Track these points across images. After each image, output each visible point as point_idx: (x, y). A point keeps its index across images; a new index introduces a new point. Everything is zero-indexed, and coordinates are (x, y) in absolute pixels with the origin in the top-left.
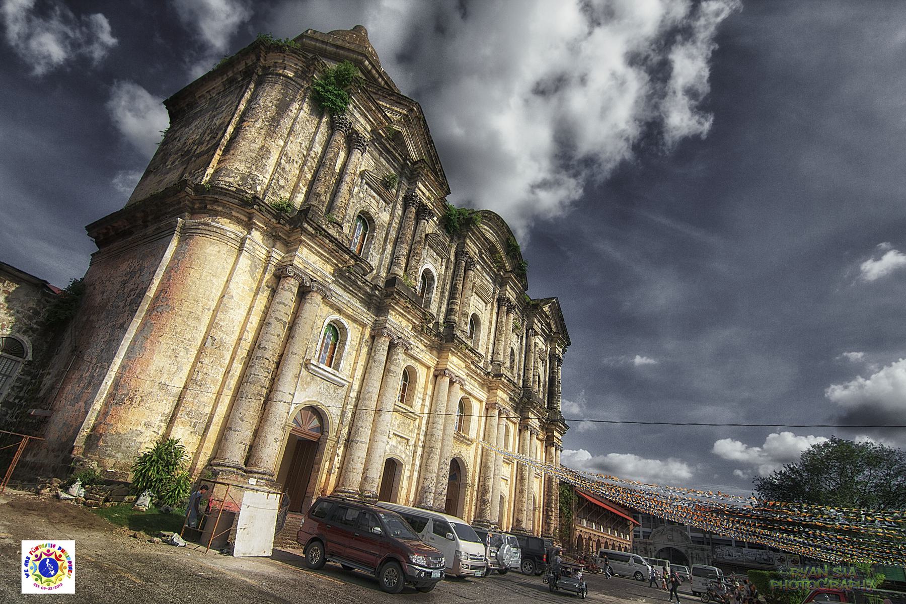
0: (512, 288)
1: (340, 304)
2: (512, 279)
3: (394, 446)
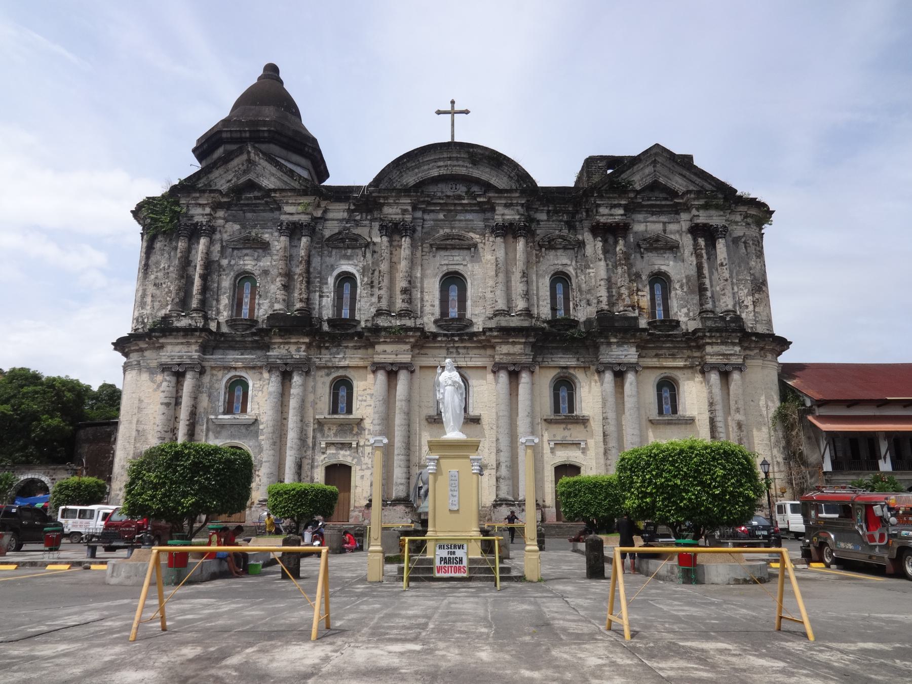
0: (506, 206)
1: (226, 364)
2: (494, 197)
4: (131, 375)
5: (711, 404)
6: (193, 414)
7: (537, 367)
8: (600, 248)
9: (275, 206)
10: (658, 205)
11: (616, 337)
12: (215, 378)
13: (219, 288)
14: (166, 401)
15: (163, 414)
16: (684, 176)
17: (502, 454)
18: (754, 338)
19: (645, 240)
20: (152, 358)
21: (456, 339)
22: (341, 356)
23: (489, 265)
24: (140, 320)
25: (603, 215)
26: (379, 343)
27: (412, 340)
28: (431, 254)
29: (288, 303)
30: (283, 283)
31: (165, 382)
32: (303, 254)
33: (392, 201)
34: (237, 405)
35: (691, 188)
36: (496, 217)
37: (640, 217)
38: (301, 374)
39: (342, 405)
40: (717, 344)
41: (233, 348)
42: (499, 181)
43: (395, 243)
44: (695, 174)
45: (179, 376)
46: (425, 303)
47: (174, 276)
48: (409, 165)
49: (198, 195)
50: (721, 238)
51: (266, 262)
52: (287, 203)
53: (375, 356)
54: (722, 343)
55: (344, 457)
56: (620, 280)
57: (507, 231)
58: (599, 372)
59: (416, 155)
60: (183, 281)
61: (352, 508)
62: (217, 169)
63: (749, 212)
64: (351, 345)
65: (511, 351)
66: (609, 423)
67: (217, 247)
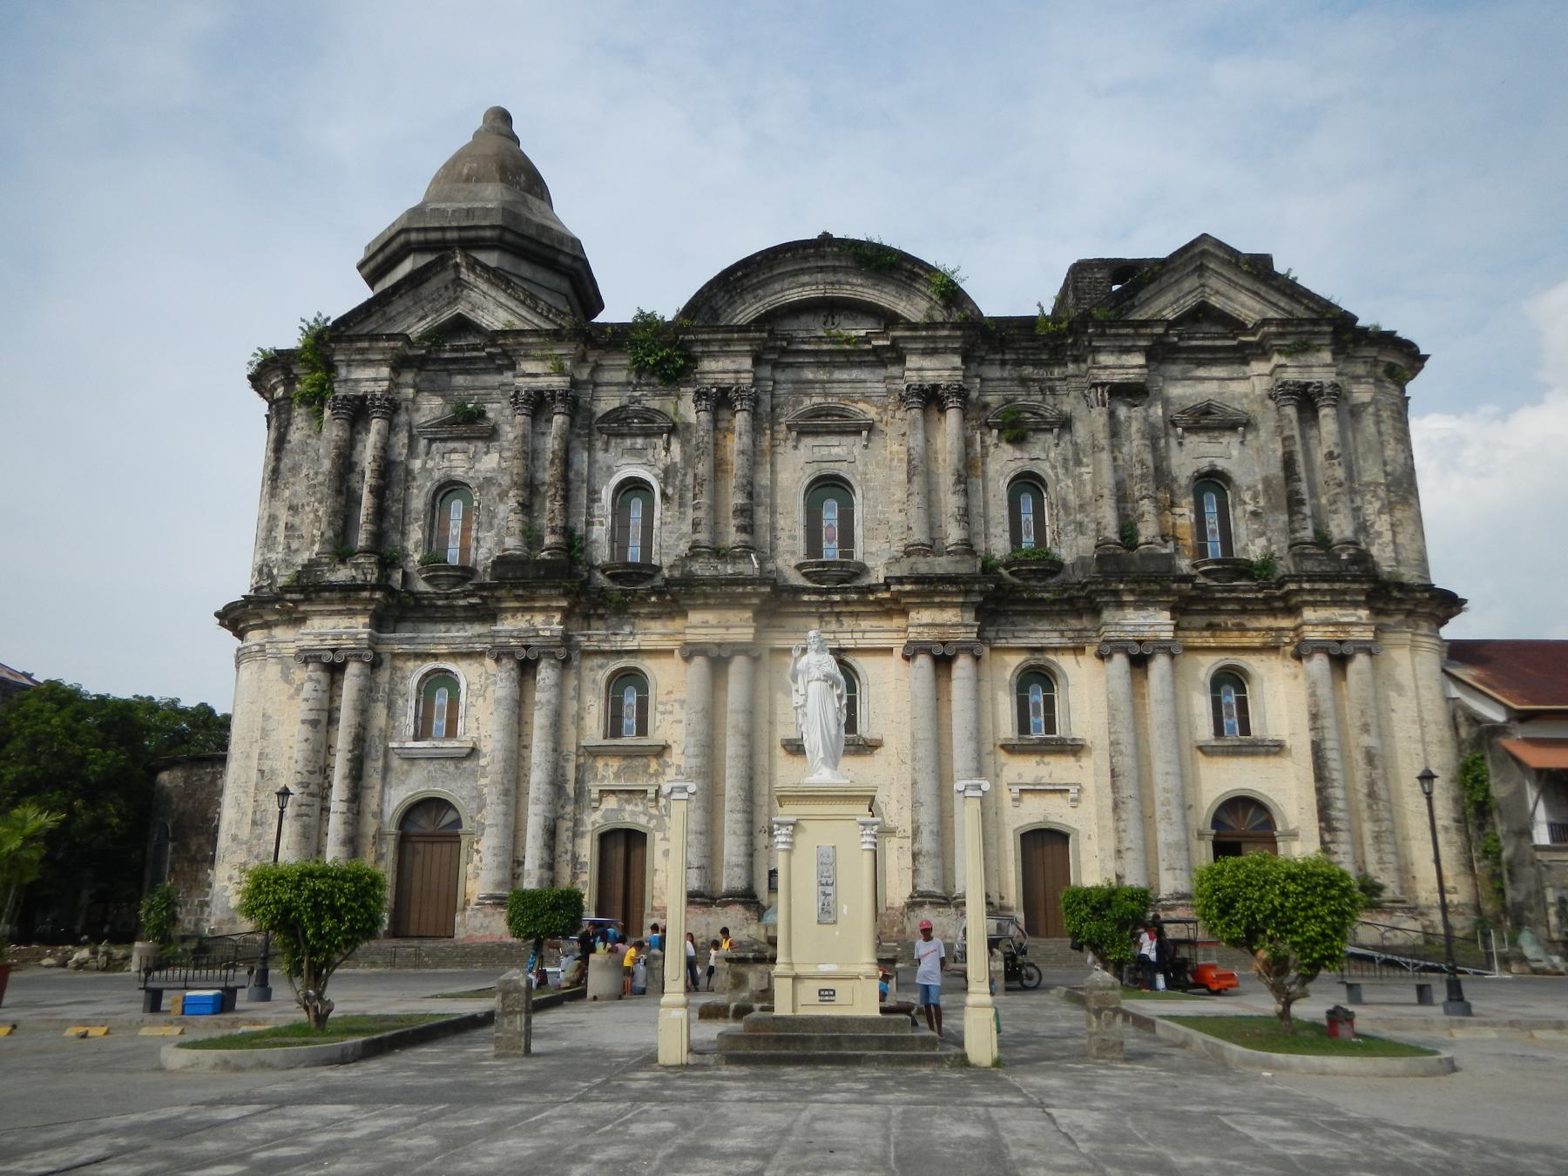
0: (926, 353)
1: (421, 648)
3: (613, 810)
4: (249, 671)
5: (1314, 717)
6: (360, 740)
7: (987, 650)
8: (1101, 428)
9: (506, 362)
10: (1208, 347)
11: (1132, 592)
12: (399, 674)
13: (405, 511)
14: (312, 716)
15: (306, 740)
16: (1257, 294)
17: (922, 809)
18: (1396, 594)
20: (288, 639)
21: (837, 598)
22: (627, 629)
23: (895, 463)
24: (265, 570)
25: (1106, 367)
26: (696, 608)
27: (755, 601)
28: (790, 443)
29: (531, 537)
30: (521, 499)
31: (308, 678)
33: (716, 349)
34: (439, 723)
35: (1271, 314)
36: (907, 373)
37: (1175, 370)
38: (554, 667)
39: (630, 721)
40: (1324, 604)
41: (433, 620)
42: (913, 308)
43: (723, 425)
44: (1278, 290)
45: (334, 670)
46: (779, 534)
47: (326, 490)
48: (746, 283)
49: (366, 345)
50: (1328, 406)
51: (490, 462)
52: (527, 357)
53: (687, 631)
54: (1334, 604)
55: (633, 815)
56: (1138, 486)
57: (931, 399)
58: (1102, 657)
59: (759, 264)
60: (342, 500)
61: (648, 910)
62: (401, 296)
63: (1380, 358)
64: (642, 611)
65: (939, 620)
66: (1121, 753)
67: (402, 438)
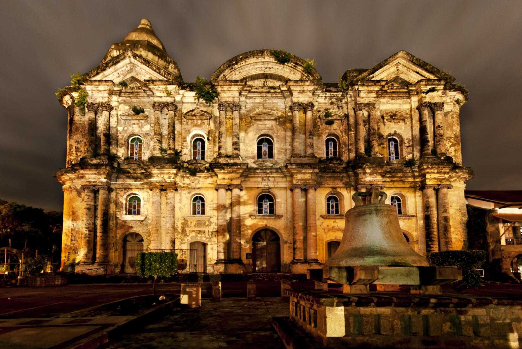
19: (387, 114)
25: (363, 98)
32: (170, 122)
